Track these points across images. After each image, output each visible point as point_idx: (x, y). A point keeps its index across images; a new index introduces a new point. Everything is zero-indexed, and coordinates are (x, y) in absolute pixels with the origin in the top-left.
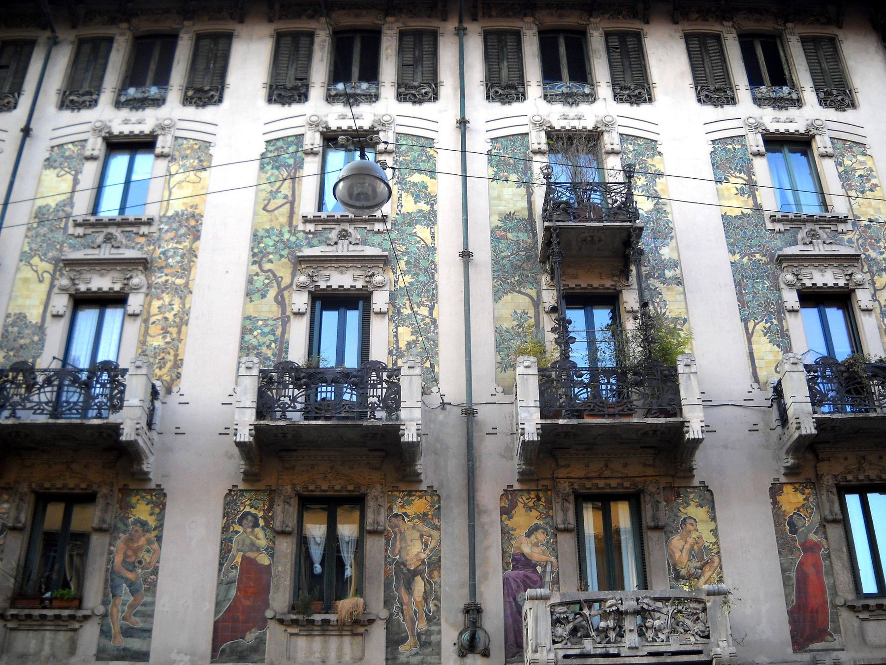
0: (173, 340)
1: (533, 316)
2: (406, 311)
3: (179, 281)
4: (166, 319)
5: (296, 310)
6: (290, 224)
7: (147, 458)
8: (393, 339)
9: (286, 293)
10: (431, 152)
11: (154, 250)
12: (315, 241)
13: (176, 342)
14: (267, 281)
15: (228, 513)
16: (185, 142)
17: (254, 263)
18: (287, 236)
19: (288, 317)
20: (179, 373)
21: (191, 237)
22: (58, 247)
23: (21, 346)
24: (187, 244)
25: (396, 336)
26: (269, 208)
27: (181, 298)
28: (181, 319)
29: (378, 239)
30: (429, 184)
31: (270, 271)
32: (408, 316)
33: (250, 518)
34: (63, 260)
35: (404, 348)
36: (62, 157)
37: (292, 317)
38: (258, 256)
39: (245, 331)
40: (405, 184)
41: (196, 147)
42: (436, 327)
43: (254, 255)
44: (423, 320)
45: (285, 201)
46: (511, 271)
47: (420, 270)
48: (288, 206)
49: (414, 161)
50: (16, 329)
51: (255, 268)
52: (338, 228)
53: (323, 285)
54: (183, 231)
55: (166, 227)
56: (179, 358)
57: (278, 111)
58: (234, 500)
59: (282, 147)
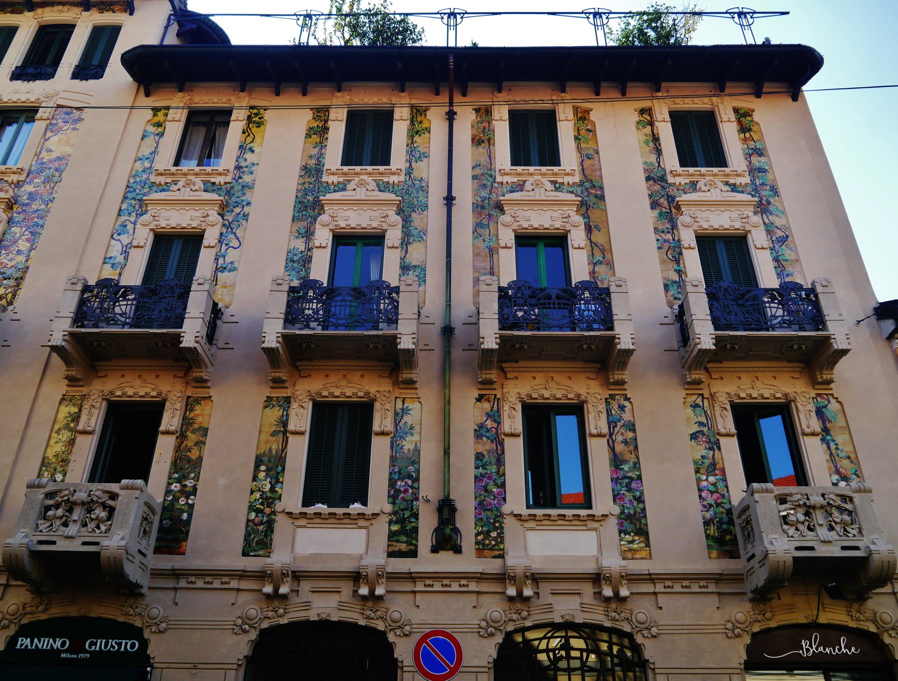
7: (207, 367)
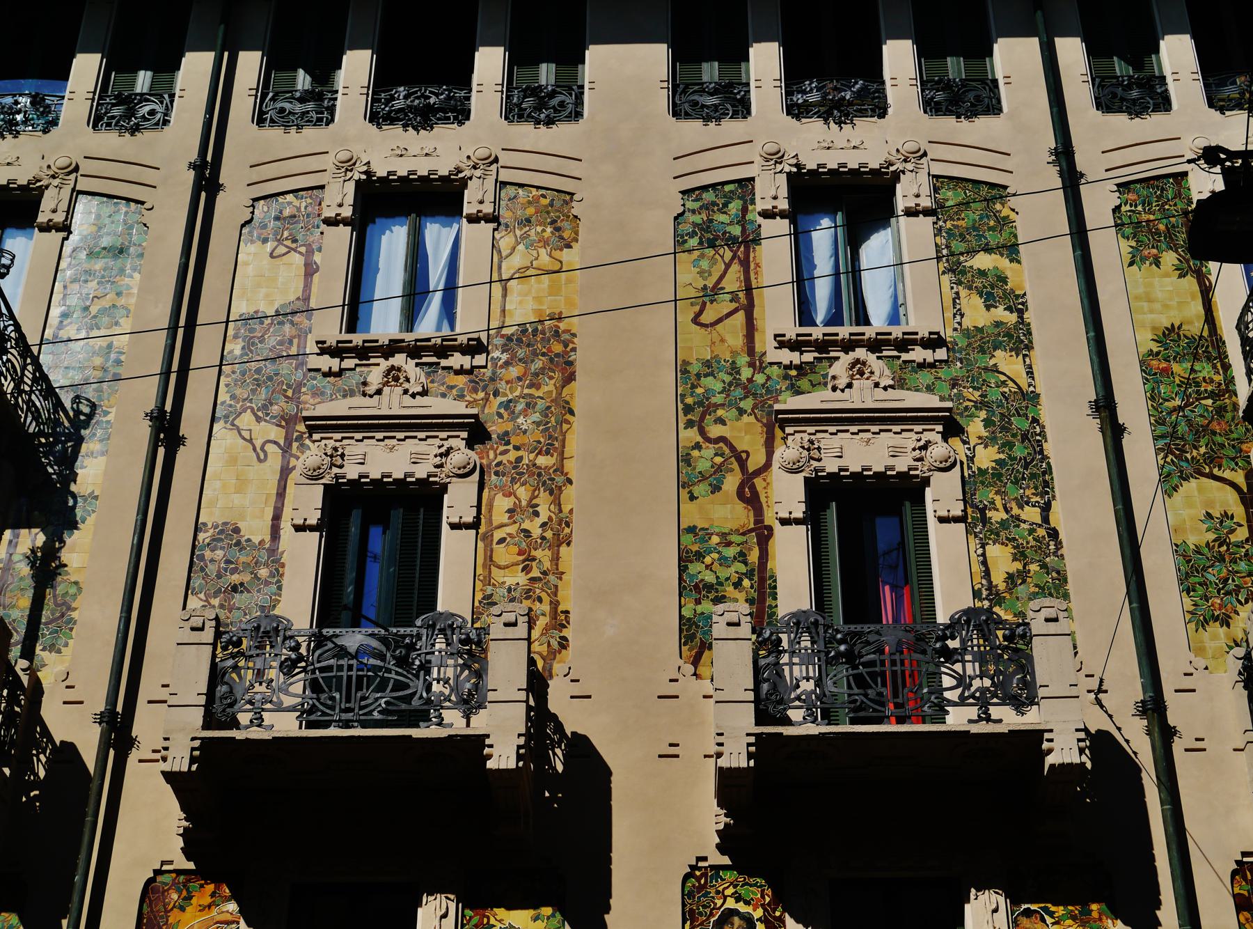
0: (545, 573)
1: (1244, 523)
2: (997, 516)
3: (542, 461)
4: (527, 533)
5: (785, 515)
6: (751, 351)
8: (977, 568)
9: (759, 482)
10: (1005, 212)
11: (487, 399)
12: (804, 383)
13: (551, 578)
14: (719, 460)
15: (691, 911)
16: (520, 191)
17: (689, 424)
18: (746, 373)
19: (770, 529)
20: (564, 638)
21: (557, 375)
22: (290, 393)
23: (235, 589)
24: (549, 386)
25: (984, 563)
26: (707, 318)
27: (551, 494)
28: (556, 535)
29: (925, 377)
30: (1008, 274)
31: (722, 439)
32: (1003, 523)
33: (737, 921)
34: (306, 419)
35: (1002, 586)
36: (277, 218)
37: (777, 527)
38: (696, 412)
39: (685, 559)
40: (963, 272)
41: (545, 202)
42: (1059, 545)
43: (688, 409)
44: (1031, 531)
45: (734, 305)
46: (1190, 438)
47: (1014, 436)
48: (741, 315)
49: (975, 228)
50: (220, 553)
51: (692, 435)
52: (846, 359)
53: (831, 466)
54: (538, 364)
55: (505, 357)
56: (561, 608)
57: (693, 131)
58: (702, 887)
59: (714, 204)
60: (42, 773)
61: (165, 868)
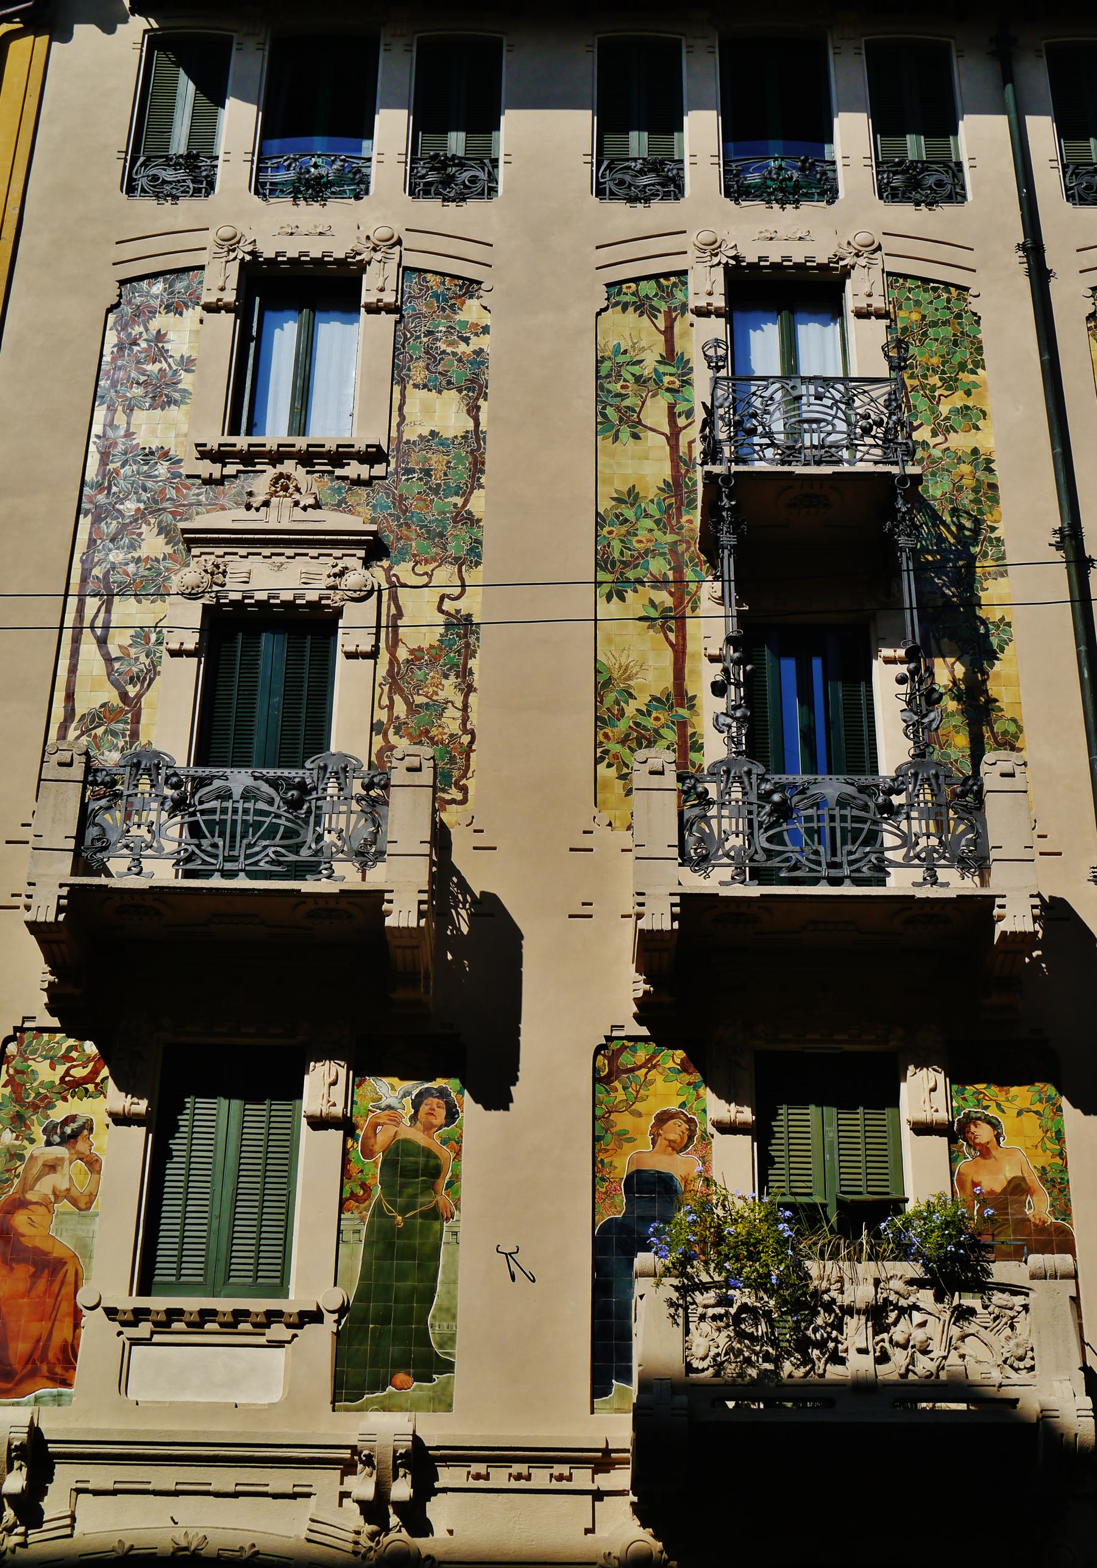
60: (465, 929)
61: (27, 1025)
